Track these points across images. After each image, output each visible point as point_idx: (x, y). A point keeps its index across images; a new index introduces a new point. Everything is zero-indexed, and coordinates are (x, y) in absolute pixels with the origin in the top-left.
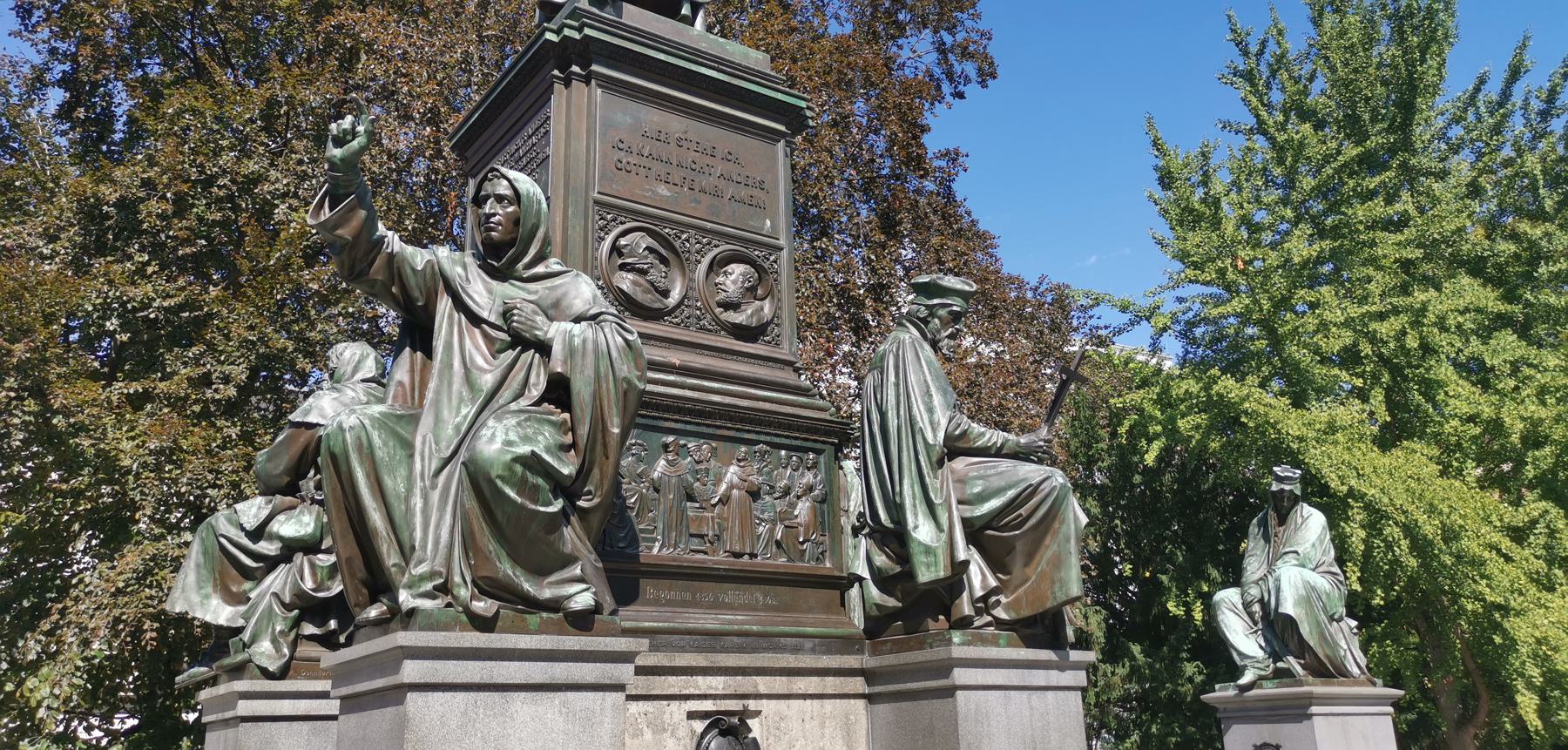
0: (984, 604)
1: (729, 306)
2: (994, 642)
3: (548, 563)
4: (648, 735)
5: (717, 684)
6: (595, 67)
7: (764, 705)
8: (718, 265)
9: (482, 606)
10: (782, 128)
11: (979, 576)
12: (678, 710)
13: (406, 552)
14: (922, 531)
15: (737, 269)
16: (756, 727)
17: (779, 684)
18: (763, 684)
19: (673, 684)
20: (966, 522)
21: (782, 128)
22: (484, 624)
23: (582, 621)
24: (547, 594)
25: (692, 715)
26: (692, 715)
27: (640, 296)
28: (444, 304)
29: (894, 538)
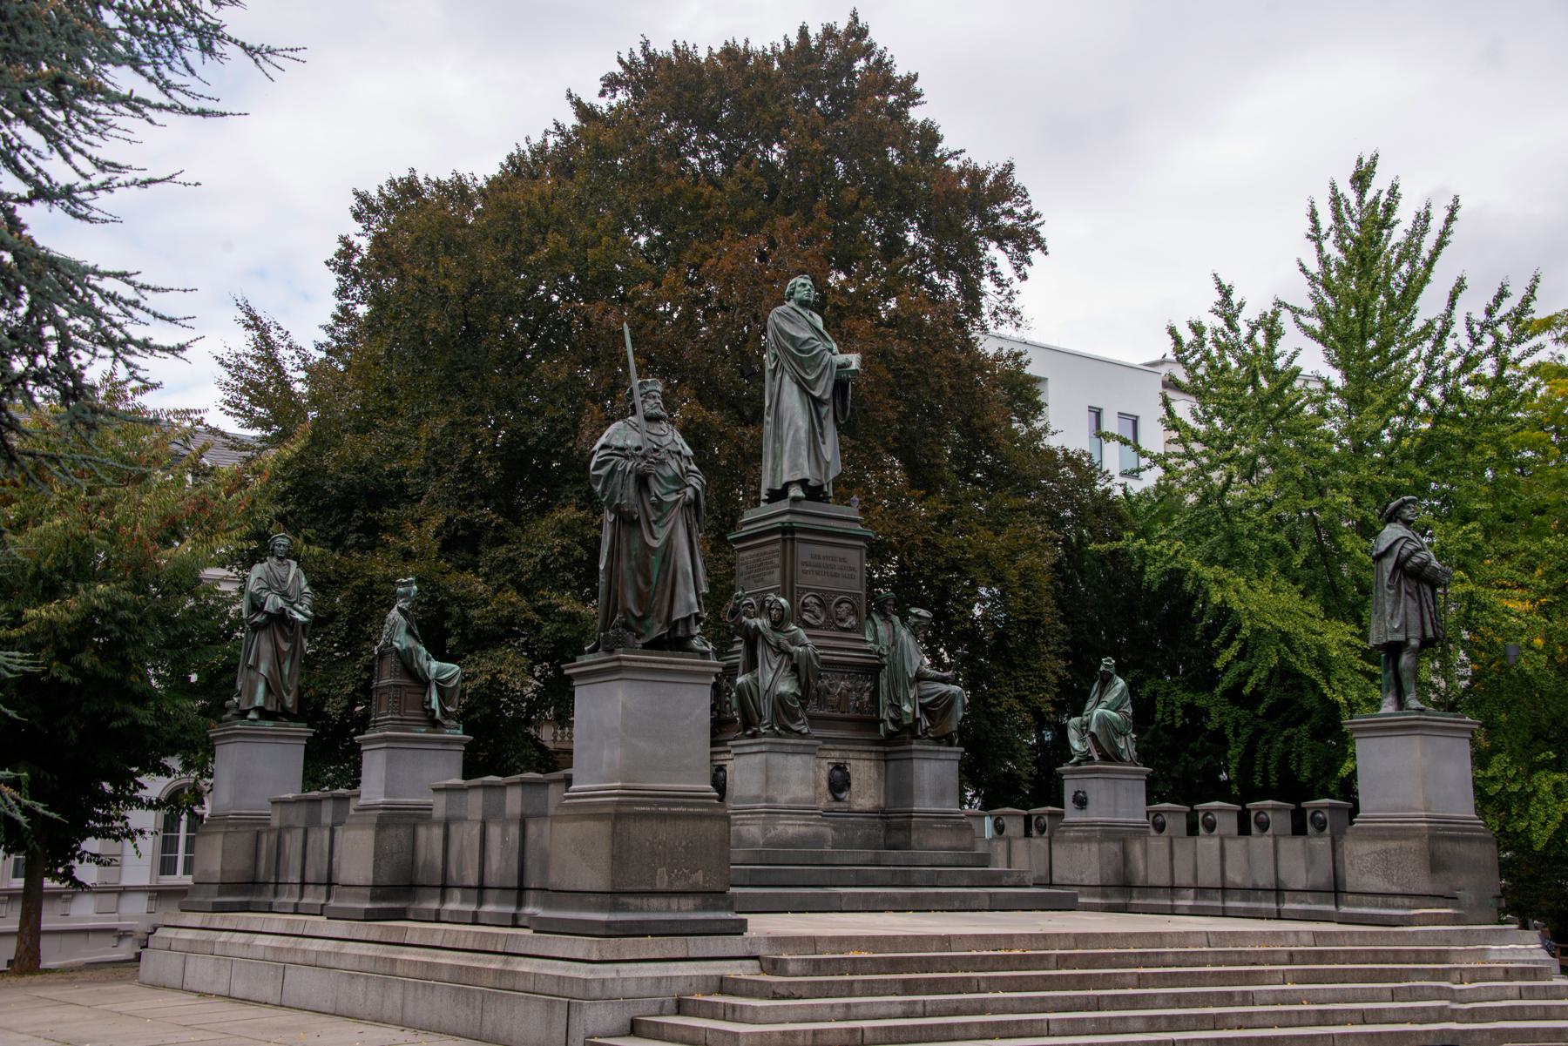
0: (925, 732)
1: (842, 620)
3: (795, 719)
5: (837, 754)
7: (853, 762)
8: (838, 604)
11: (925, 723)
12: (824, 763)
13: (761, 717)
14: (907, 708)
15: (844, 606)
18: (851, 755)
19: (824, 754)
22: (778, 735)
28: (760, 640)
29: (897, 708)
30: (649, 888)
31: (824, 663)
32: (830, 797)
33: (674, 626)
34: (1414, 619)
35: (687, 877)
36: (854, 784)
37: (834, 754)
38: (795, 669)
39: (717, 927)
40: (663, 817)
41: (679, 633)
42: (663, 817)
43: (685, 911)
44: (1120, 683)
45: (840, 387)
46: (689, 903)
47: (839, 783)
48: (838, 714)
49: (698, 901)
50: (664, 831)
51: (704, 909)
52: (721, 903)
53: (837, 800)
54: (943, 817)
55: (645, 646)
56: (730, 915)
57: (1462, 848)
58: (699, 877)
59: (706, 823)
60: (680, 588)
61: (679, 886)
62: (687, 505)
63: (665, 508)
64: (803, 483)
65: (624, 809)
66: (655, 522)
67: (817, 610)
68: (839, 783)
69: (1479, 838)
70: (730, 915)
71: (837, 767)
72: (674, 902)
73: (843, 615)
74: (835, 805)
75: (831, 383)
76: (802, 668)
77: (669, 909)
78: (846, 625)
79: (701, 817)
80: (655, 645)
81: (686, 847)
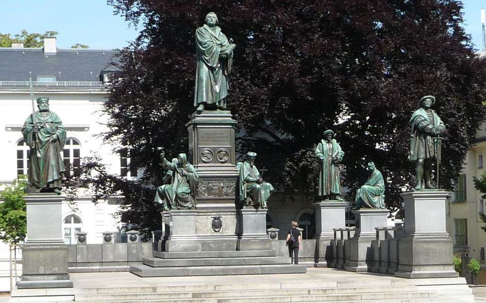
2: (251, 208)
4: (206, 220)
5: (215, 214)
6: (198, 126)
7: (223, 216)
9: (179, 207)
10: (231, 126)
16: (221, 218)
17: (224, 213)
18: (222, 213)
19: (209, 214)
20: (247, 192)
21: (231, 126)
22: (179, 209)
23: (190, 208)
24: (186, 205)
25: (212, 217)
26: (212, 217)
27: (206, 161)
30: (37, 273)
31: (200, 177)
32: (212, 230)
33: (48, 184)
34: (422, 150)
35: (51, 269)
36: (224, 225)
37: (213, 214)
38: (188, 182)
39: (61, 286)
40: (41, 250)
41: (50, 187)
42: (41, 250)
43: (51, 280)
44: (377, 172)
45: (223, 60)
46: (53, 277)
47: (217, 225)
48: (218, 197)
49: (55, 277)
50: (42, 254)
51: (55, 280)
52: (64, 277)
53: (216, 231)
54: (255, 237)
55: (41, 192)
56: (67, 281)
57: (432, 246)
58: (56, 270)
59: (59, 251)
60: (50, 171)
61: (48, 272)
62: (54, 141)
63: (43, 144)
64: (205, 104)
65: (26, 248)
66: (41, 148)
67: (209, 156)
68: (217, 225)
69: (443, 241)
70: (67, 281)
71: (215, 218)
72: (46, 277)
73: (222, 156)
74: (216, 234)
75: (217, 60)
76: (191, 182)
77: (44, 280)
78: (223, 160)
79: (56, 249)
80: (43, 191)
81: (51, 259)
